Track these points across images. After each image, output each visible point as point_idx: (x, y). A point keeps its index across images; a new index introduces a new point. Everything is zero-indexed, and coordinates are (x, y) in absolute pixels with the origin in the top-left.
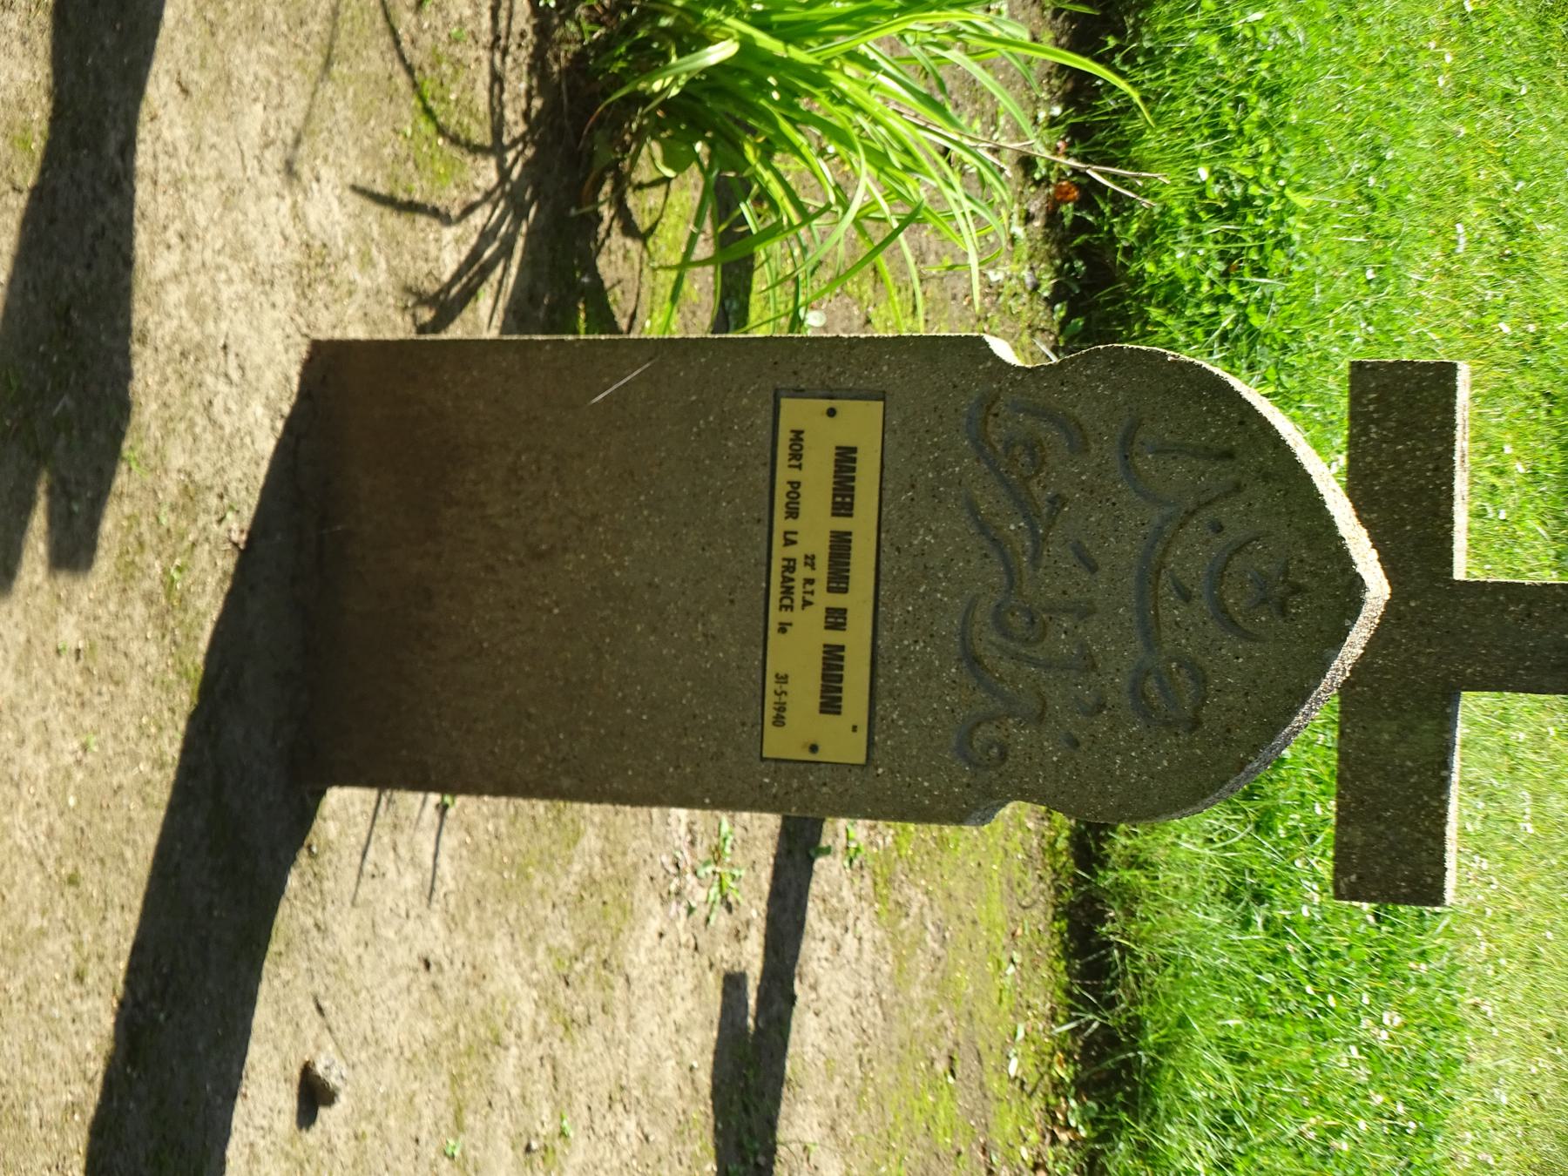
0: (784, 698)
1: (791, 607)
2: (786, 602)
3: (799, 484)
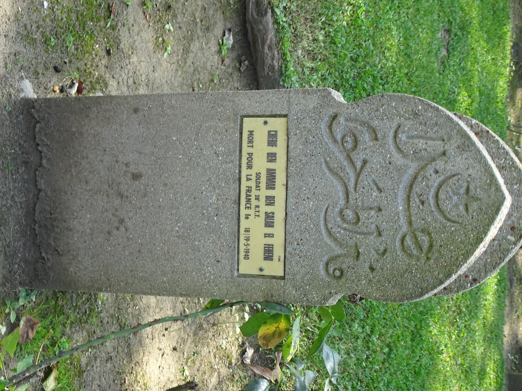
0: (248, 247)
1: (250, 208)
2: (248, 205)
3: (252, 154)
